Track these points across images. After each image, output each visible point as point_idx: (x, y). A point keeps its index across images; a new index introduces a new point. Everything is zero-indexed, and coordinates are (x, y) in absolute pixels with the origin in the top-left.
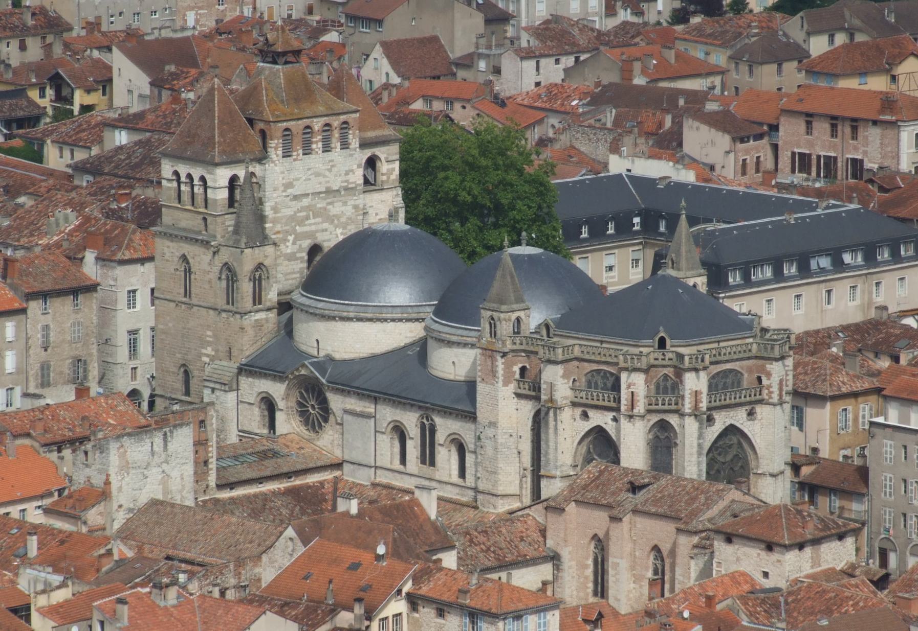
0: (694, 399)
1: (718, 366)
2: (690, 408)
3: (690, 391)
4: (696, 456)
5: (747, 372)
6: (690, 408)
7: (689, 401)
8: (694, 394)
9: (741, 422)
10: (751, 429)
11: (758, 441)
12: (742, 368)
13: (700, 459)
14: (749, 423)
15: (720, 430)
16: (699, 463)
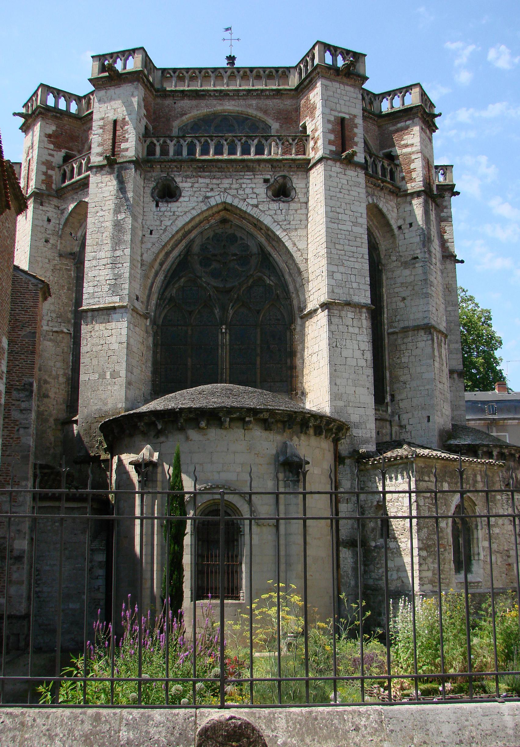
0: (109, 136)
1: (203, 103)
2: (100, 155)
3: (101, 123)
4: (108, 247)
5: (277, 119)
6: (100, 155)
7: (100, 139)
8: (110, 127)
9: (255, 202)
10: (281, 218)
11: (301, 245)
12: (265, 112)
13: (118, 253)
14: (274, 206)
15: (195, 213)
16: (114, 263)
